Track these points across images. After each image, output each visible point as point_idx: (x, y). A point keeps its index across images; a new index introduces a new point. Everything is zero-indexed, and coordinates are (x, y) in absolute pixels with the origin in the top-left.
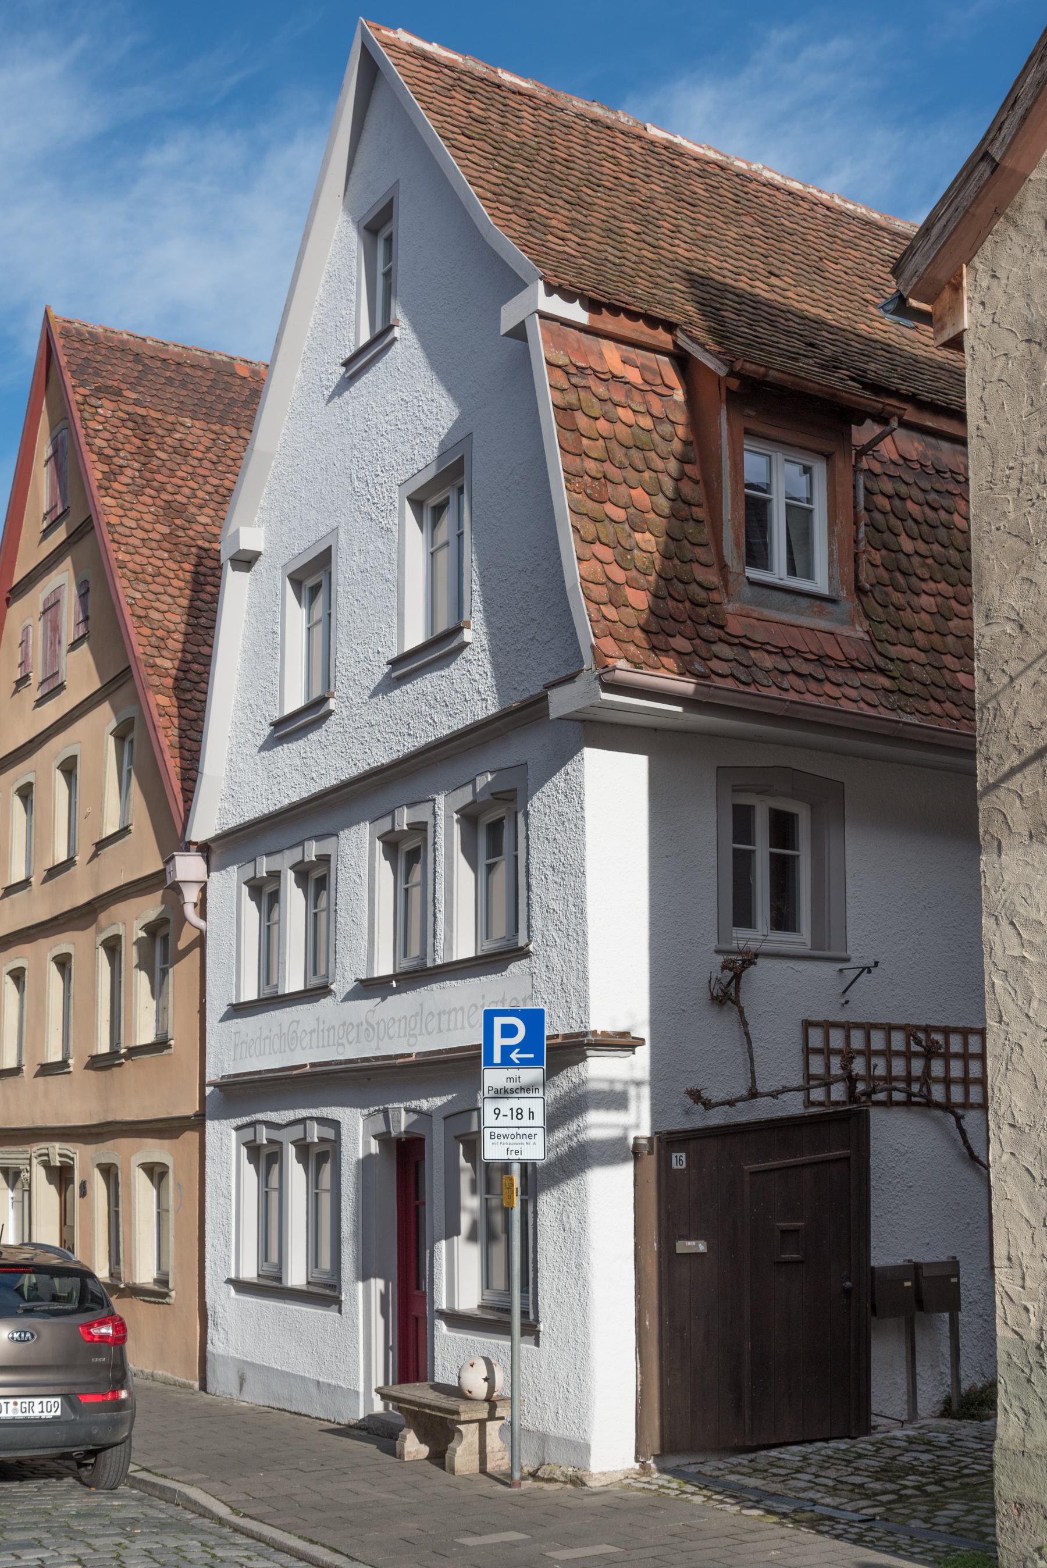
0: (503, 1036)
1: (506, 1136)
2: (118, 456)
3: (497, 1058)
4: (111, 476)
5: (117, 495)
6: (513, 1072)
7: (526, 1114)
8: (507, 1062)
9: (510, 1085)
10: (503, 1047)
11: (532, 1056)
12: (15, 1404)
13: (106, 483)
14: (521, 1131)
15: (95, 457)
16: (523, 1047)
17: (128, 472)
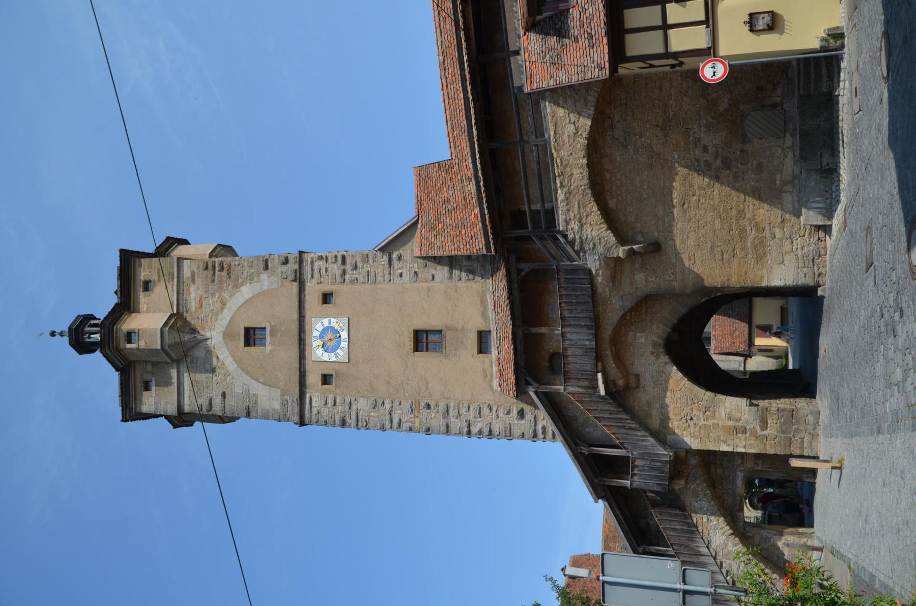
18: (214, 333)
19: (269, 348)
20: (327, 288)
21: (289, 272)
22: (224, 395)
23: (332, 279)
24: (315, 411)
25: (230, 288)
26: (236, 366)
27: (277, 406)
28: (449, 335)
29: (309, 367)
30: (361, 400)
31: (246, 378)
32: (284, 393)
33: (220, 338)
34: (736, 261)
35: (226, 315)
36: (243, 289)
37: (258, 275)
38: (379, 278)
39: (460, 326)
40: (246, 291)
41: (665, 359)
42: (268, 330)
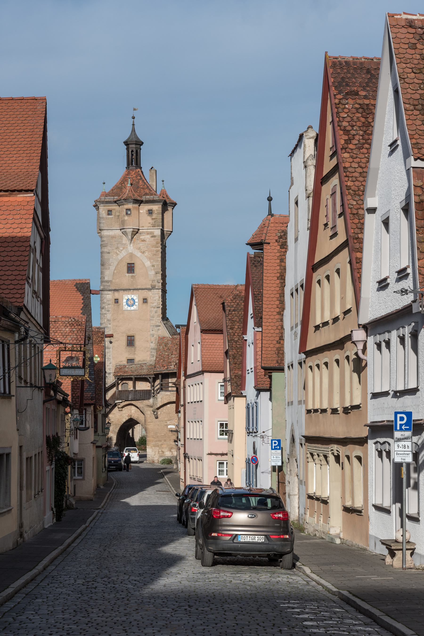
0: (400, 420)
1: (401, 454)
2: (353, 129)
3: (398, 428)
4: (348, 142)
5: (350, 151)
6: (403, 433)
7: (406, 447)
8: (401, 429)
9: (402, 437)
10: (400, 424)
11: (408, 427)
12: (250, 537)
13: (346, 146)
14: (405, 452)
15: (342, 132)
16: (406, 424)
17: (357, 137)
18: (132, 248)
19: (127, 275)
20: (149, 301)
21: (155, 284)
22: (109, 253)
23: (152, 303)
24: (105, 296)
25: (149, 256)
26: (120, 259)
27: (106, 279)
28: (133, 349)
29: (121, 292)
30: (110, 315)
31: (116, 263)
32: (111, 281)
33: (130, 251)
34: (153, 439)
35: (138, 254)
36: (149, 262)
37: (154, 269)
38: (152, 322)
39: (136, 353)
40: (148, 264)
41: (127, 418)
42: (133, 274)
